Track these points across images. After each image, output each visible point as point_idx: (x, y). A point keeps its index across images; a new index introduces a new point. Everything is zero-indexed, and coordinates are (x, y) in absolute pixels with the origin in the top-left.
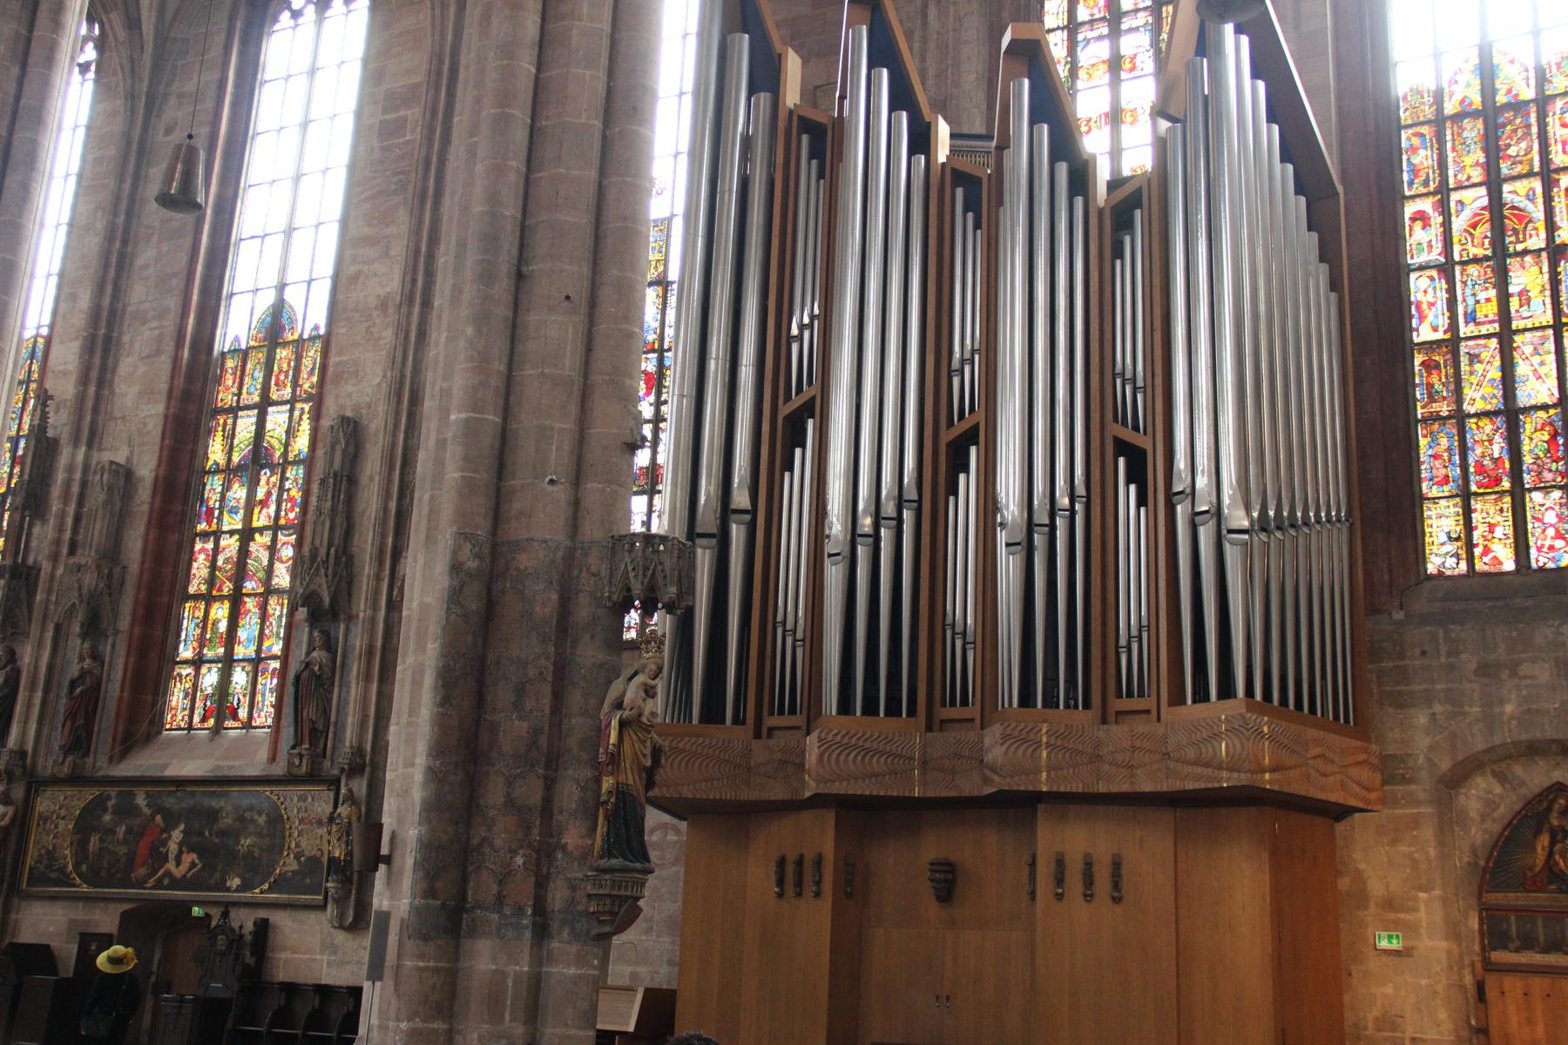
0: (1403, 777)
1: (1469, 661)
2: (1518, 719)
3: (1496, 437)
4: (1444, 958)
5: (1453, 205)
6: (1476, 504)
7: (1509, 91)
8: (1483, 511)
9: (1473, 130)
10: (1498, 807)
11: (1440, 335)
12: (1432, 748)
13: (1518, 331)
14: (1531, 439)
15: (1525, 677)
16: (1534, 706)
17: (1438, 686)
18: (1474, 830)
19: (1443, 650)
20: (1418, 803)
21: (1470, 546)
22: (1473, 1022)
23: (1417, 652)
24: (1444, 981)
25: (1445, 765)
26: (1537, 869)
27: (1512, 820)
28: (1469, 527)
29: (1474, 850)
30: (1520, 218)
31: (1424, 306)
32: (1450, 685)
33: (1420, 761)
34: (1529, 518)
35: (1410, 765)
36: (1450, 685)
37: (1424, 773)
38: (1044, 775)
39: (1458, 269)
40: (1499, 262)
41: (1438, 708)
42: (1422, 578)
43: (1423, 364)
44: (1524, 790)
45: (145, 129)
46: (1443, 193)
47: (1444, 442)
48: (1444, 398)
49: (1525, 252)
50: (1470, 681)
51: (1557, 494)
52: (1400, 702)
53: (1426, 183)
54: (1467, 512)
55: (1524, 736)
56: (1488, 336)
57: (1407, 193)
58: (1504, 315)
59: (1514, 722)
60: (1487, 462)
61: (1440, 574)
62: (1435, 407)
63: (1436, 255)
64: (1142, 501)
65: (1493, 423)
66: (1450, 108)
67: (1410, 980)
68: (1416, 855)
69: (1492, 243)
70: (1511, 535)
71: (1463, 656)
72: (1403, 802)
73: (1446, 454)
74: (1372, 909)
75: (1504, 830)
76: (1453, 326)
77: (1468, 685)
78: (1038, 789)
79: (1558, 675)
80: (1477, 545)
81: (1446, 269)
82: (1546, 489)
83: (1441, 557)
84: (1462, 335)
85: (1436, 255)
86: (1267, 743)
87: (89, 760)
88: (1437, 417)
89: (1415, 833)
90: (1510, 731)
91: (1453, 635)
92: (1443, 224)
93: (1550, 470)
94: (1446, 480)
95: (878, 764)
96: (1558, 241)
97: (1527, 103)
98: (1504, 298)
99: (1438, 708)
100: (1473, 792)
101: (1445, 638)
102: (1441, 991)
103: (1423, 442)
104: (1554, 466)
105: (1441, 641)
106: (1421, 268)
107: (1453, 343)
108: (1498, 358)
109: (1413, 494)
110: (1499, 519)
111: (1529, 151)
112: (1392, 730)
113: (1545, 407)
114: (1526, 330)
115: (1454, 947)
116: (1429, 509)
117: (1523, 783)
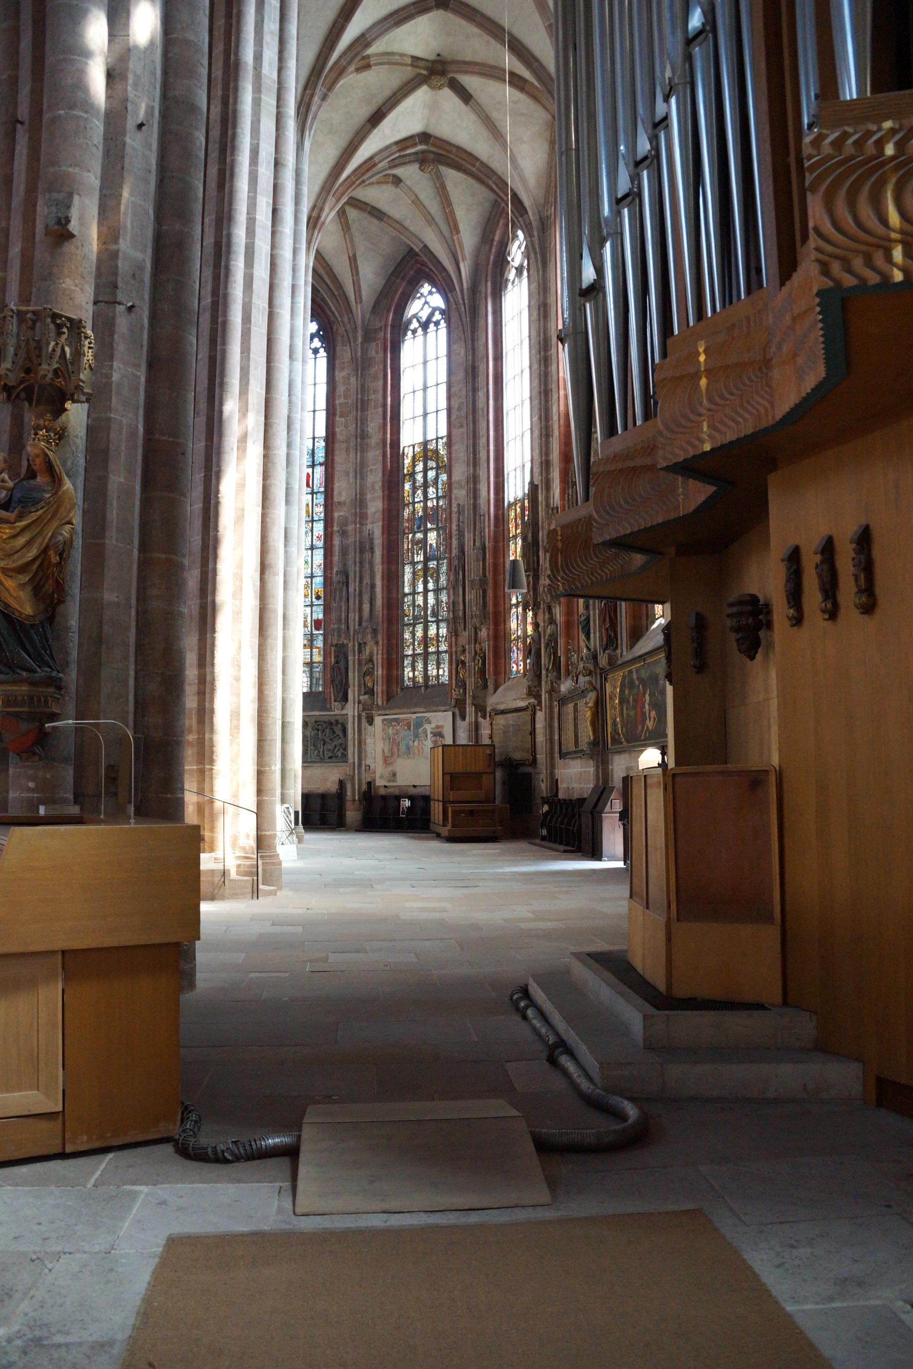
87: (619, 651)
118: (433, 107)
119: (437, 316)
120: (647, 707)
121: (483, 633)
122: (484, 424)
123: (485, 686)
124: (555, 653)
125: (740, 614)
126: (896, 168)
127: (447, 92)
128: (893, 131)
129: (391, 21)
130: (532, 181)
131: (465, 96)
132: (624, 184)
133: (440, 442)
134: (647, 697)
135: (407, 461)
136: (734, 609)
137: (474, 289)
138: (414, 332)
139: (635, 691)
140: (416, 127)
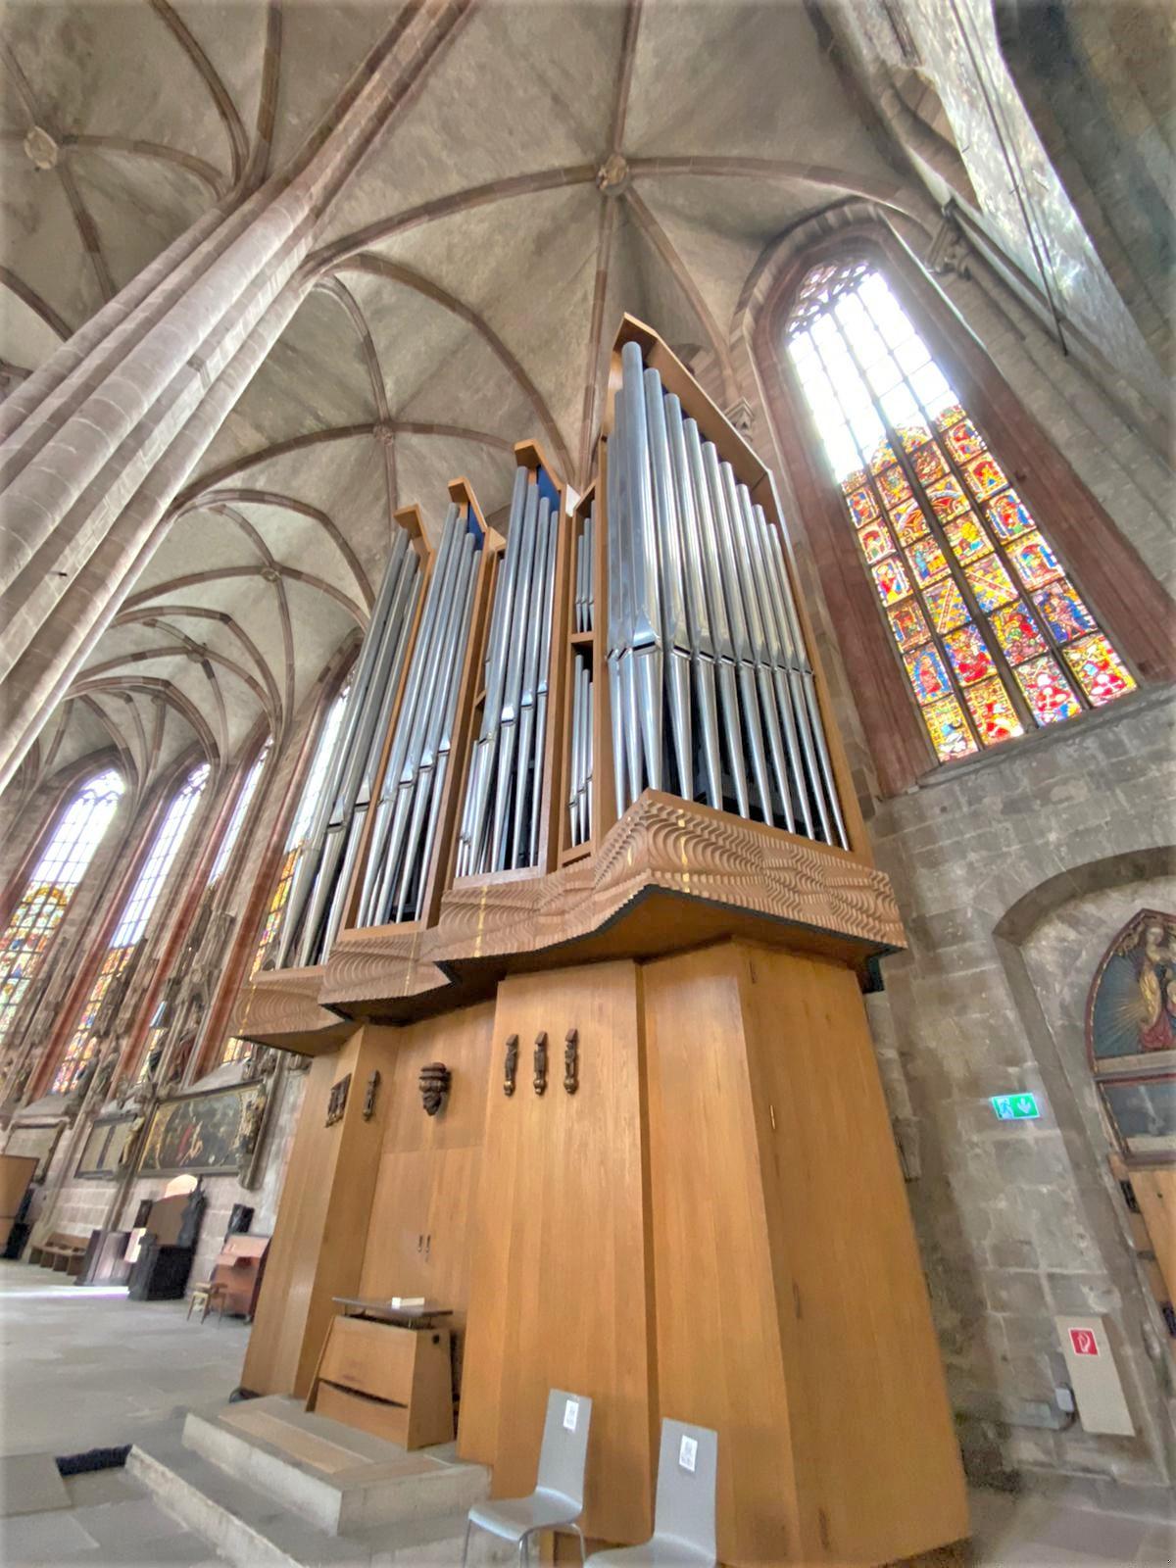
0: (954, 935)
1: (993, 802)
2: (1068, 845)
3: (972, 640)
4: (1062, 1151)
5: (892, 518)
6: (971, 695)
7: (913, 443)
8: (977, 700)
9: (895, 475)
10: (1078, 955)
11: (904, 594)
12: (978, 898)
13: (967, 566)
14: (1003, 631)
15: (1061, 801)
16: (1081, 828)
17: (968, 836)
18: (1058, 987)
19: (963, 800)
20: (979, 960)
21: (974, 727)
22: (1131, 1243)
23: (937, 810)
24: (1074, 1187)
25: (998, 912)
26: (1155, 1019)
27: (1101, 964)
28: (968, 713)
29: (1065, 1009)
30: (945, 502)
31: (888, 582)
32: (979, 831)
33: (969, 915)
34: (1023, 689)
35: (959, 921)
36: (979, 831)
37: (976, 926)
38: (479, 940)
39: (907, 552)
40: (938, 532)
41: (972, 856)
42: (936, 764)
43: (896, 617)
44: (1103, 930)
45: (278, 761)
46: (884, 517)
47: (928, 661)
48: (919, 632)
49: (956, 518)
50: (999, 822)
51: (1043, 662)
52: (933, 861)
53: (870, 515)
54: (963, 702)
55: (1080, 861)
56: (944, 579)
57: (858, 527)
58: (952, 560)
59: (1064, 849)
60: (969, 661)
61: (953, 759)
62: (913, 641)
63: (889, 550)
64: (591, 679)
65: (966, 633)
66: (875, 472)
67: (1026, 1187)
68: (992, 1021)
69: (929, 525)
70: (1010, 707)
71: (986, 801)
72: (961, 963)
73: (932, 670)
74: (956, 1095)
75: (1095, 980)
76: (913, 584)
77: (1000, 826)
78: (470, 956)
79: (1098, 788)
80: (981, 725)
81: (899, 555)
82: (1032, 661)
83: (949, 738)
84: (921, 587)
85: (889, 550)
86: (683, 840)
87: (180, 1085)
88: (917, 647)
89: (984, 995)
90: (1062, 859)
91: (970, 784)
92: (889, 531)
93: (1029, 646)
94: (936, 688)
95: (376, 969)
96: (979, 501)
97: (928, 444)
98: (949, 552)
99: (972, 856)
100: (1044, 943)
101: (962, 789)
102: (1072, 1200)
103: (910, 668)
104: (1032, 642)
105: (958, 793)
106: (879, 562)
107: (917, 595)
108: (956, 589)
109: (910, 705)
110: (995, 698)
111: (938, 464)
112: (930, 889)
113: (1008, 605)
114: (973, 563)
115: (1073, 1135)
116: (928, 713)
117: (1101, 922)
118: (183, 669)
119: (112, 797)
120: (195, 1136)
121: (38, 1051)
122: (118, 883)
123: (18, 1100)
124: (108, 1078)
125: (433, 1078)
126: (686, 834)
127: (199, 666)
128: (683, 816)
129: (185, 611)
130: (231, 741)
131: (210, 674)
132: (408, 775)
133: (70, 886)
134: (198, 1129)
135: (30, 892)
136: (430, 1074)
137: (153, 790)
138: (86, 801)
139: (187, 1122)
140: (164, 676)
